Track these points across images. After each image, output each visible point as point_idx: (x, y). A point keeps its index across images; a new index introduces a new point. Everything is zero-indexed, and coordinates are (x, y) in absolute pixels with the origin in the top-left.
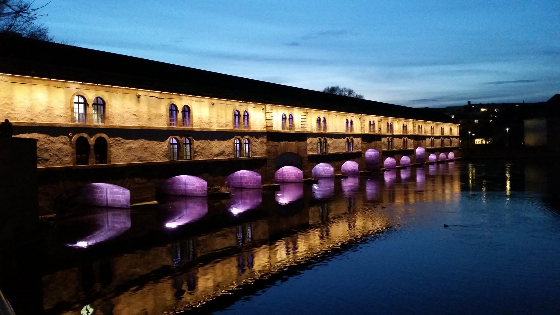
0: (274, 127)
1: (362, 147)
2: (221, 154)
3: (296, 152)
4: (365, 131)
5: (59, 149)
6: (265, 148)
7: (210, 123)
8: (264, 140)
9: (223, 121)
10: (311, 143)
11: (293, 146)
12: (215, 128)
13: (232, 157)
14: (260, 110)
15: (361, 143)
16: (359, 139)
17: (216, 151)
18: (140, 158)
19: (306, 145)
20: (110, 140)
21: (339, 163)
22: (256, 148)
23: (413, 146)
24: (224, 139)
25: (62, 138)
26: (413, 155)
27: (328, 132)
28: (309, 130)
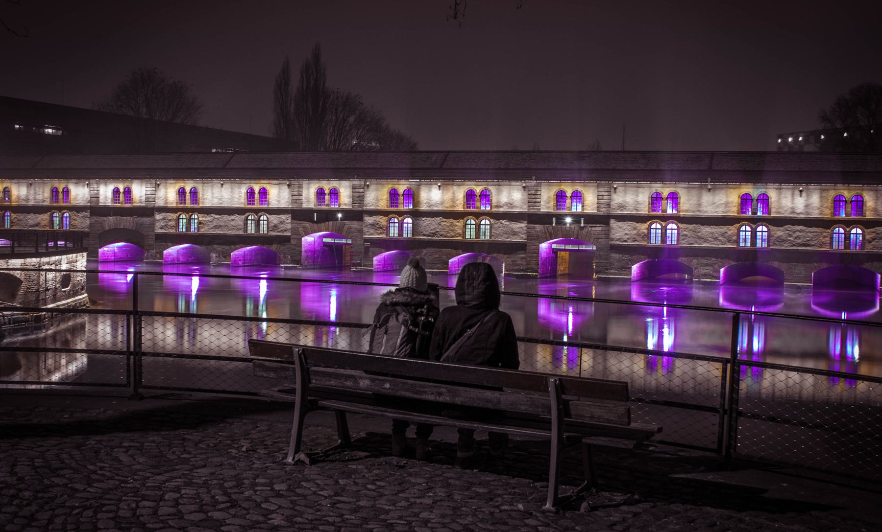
0: (101, 201)
1: (291, 228)
2: (37, 225)
3: (134, 229)
4: (303, 205)
6: (88, 222)
8: (88, 214)
10: (164, 219)
11: (128, 222)
12: (31, 203)
13: (48, 229)
14: (84, 186)
15: (291, 223)
17: (31, 222)
19: (154, 222)
21: (227, 248)
22: (76, 222)
23: (524, 236)
26: (524, 256)
27: (201, 205)
28: (160, 203)
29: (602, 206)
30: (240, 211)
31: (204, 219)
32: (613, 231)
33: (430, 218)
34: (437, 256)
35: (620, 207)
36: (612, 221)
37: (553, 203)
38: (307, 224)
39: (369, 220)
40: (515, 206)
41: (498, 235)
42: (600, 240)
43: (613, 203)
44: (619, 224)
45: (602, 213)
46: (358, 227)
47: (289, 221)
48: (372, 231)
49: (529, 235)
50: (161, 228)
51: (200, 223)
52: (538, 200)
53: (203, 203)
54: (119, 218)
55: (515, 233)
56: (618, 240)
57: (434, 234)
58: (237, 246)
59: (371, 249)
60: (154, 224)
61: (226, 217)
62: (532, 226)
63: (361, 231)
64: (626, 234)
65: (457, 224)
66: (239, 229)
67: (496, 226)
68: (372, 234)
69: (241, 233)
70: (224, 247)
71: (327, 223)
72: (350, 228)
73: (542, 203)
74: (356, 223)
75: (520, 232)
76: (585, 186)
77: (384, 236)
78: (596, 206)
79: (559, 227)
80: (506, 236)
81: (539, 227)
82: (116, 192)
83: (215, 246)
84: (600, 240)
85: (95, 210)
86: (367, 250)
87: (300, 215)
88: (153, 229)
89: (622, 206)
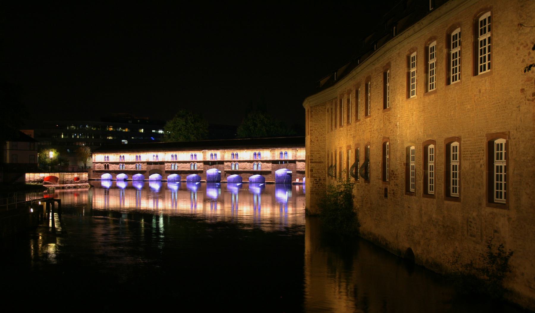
2: (132, 168)
5: (102, 166)
7: (129, 160)
8: (146, 164)
9: (133, 159)
10: (168, 165)
11: (157, 167)
12: (130, 161)
13: (135, 170)
15: (204, 166)
16: (202, 164)
17: (130, 168)
18: (114, 169)
19: (165, 167)
20: (109, 164)
21: (185, 175)
23: (271, 168)
24: (133, 164)
25: (103, 164)
26: (271, 175)
28: (166, 160)
29: (294, 157)
30: (189, 162)
31: (179, 165)
32: (297, 166)
33: (243, 163)
34: (245, 176)
35: (299, 157)
36: (297, 163)
37: (279, 156)
38: (208, 166)
39: (226, 164)
40: (268, 158)
41: (263, 168)
42: (293, 169)
43: (297, 156)
44: (299, 163)
45: (293, 159)
46: (223, 167)
47: (203, 165)
48: (227, 168)
49: (272, 168)
50: (167, 169)
51: (178, 166)
52: (275, 155)
53: (178, 159)
54: (155, 165)
55: (268, 168)
56: (299, 169)
57: (244, 169)
58: (188, 174)
59: (227, 174)
60: (165, 167)
61: (185, 164)
62: (273, 164)
63: (224, 168)
64: (301, 167)
65: (251, 165)
66: (189, 168)
67: (262, 165)
68: (227, 169)
69: (189, 170)
70: (184, 175)
71: (214, 165)
72: (220, 167)
73: (276, 156)
74: (222, 165)
75: (269, 167)
76: (288, 150)
77: (230, 170)
78: (292, 157)
79: (281, 164)
80: (266, 168)
81: (275, 165)
82: (154, 156)
83: (182, 174)
84: (293, 169)
85: (149, 163)
86: (225, 174)
87: (206, 163)
88: (164, 169)
89: (300, 157)
